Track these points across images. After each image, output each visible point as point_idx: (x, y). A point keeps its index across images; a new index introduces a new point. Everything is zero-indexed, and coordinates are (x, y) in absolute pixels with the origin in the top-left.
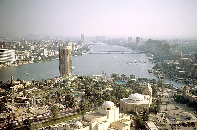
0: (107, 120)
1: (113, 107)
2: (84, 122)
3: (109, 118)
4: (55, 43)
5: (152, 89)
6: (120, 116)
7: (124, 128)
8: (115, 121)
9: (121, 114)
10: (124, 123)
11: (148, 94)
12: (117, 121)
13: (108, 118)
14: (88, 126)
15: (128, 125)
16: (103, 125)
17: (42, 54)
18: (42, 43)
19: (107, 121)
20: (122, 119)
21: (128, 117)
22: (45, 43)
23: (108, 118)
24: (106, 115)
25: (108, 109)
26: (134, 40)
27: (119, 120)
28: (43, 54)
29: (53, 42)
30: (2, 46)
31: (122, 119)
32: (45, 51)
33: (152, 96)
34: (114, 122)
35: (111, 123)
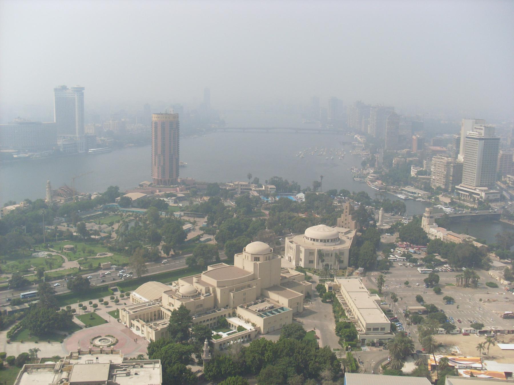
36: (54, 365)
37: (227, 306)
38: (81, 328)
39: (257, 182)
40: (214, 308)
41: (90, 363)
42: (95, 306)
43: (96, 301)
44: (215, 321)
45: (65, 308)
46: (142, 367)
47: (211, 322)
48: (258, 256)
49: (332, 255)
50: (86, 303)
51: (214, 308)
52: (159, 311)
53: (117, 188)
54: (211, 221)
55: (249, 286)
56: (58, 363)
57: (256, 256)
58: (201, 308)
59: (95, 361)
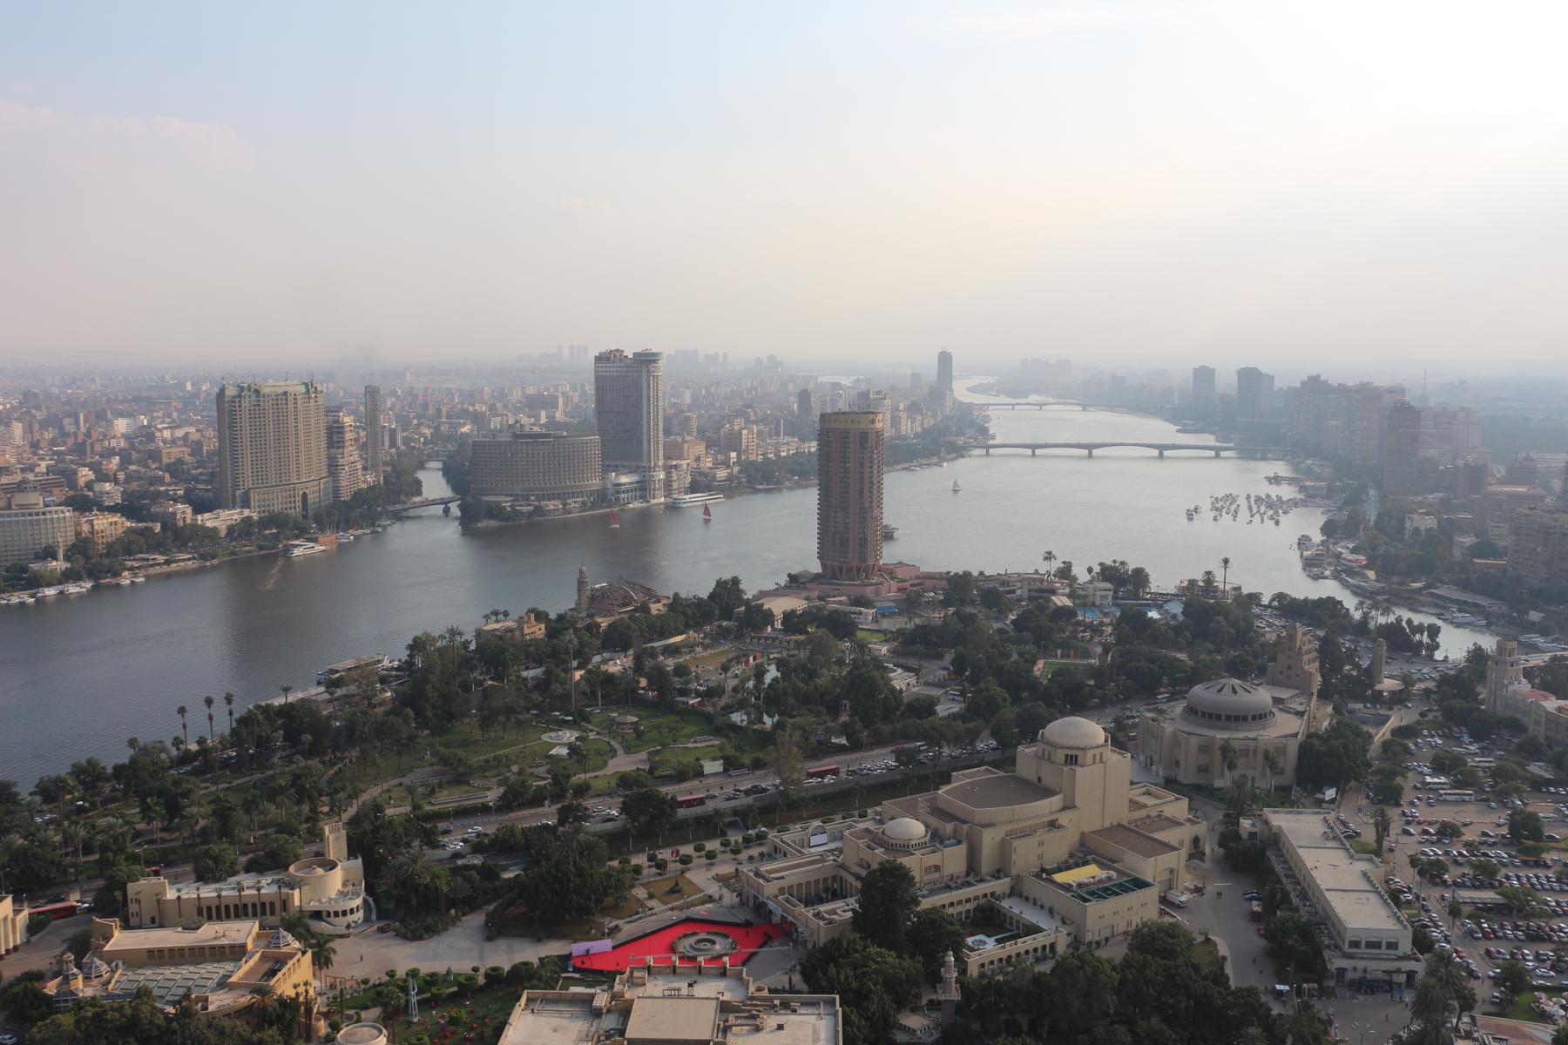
0: (1063, 819)
1: (1097, 752)
2: (934, 822)
3: (1074, 807)
4: (804, 396)
6: (1131, 801)
8: (1107, 825)
9: (1136, 794)
10: (1158, 836)
11: (1298, 683)
12: (1119, 825)
13: (1068, 806)
14: (959, 842)
15: (1174, 849)
16: (1041, 844)
17: (733, 455)
20: (1141, 814)
21: (1178, 807)
25: (1072, 760)
26: (1226, 381)
28: (739, 456)
30: (543, 414)
31: (1141, 814)
34: (1098, 826)
35: (1083, 834)
36: (593, 996)
37: (998, 871)
39: (1065, 572)
41: (674, 995)
42: (686, 860)
43: (687, 850)
44: (969, 906)
45: (615, 863)
46: (794, 1011)
47: (960, 908)
48: (1074, 753)
49: (1255, 755)
50: (665, 854)
51: (968, 874)
52: (834, 878)
53: (735, 581)
54: (959, 665)
55: (1053, 825)
57: (1070, 752)
58: (937, 875)
59: (685, 992)
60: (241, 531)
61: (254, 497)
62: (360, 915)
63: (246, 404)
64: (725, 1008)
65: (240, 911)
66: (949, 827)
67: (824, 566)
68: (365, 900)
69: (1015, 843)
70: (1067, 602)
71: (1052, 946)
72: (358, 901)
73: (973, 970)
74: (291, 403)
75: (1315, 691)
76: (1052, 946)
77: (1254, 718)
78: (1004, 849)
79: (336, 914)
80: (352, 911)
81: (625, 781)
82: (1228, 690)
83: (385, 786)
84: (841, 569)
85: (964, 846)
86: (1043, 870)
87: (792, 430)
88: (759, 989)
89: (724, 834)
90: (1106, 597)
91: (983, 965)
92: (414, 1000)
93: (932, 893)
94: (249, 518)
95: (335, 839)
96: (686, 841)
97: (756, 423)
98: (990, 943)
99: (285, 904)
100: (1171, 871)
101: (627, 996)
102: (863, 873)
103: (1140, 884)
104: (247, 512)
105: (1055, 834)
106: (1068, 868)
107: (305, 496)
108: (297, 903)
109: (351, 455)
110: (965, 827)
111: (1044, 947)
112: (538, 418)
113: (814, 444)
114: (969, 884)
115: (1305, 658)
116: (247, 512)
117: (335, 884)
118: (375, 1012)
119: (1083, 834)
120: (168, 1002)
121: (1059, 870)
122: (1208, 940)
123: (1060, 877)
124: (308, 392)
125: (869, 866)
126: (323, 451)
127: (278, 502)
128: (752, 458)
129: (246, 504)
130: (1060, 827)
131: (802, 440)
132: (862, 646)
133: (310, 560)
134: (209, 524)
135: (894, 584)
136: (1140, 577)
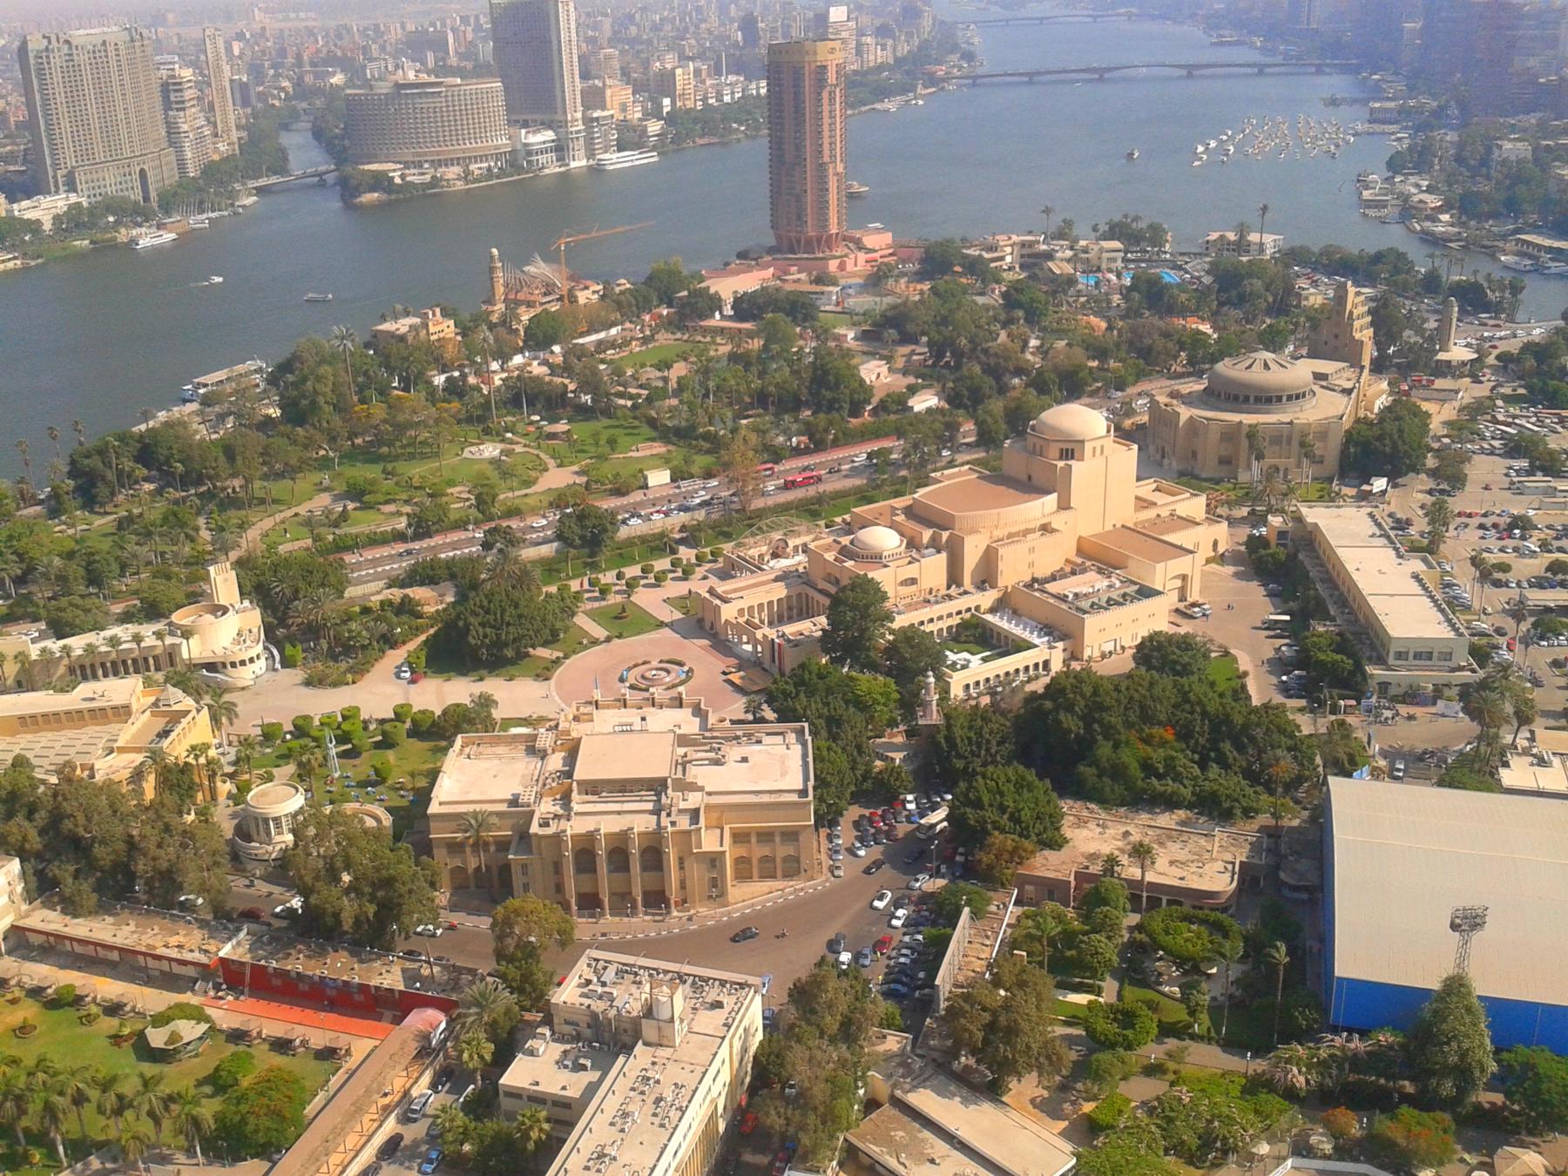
1: (1098, 444)
3: (1068, 508)
4: (748, 24)
5: (1372, 324)
7: (1160, 567)
8: (1109, 527)
10: (1165, 538)
11: (1347, 352)
14: (939, 552)
17: (667, 101)
18: (668, 27)
19: (1054, 526)
20: (1150, 514)
22: (686, 29)
23: (1064, 505)
24: (1048, 492)
27: (1131, 517)
28: (673, 103)
29: (732, 20)
31: (1150, 514)
32: (683, 77)
33: (1366, 371)
38: (595, 642)
40: (949, 587)
43: (632, 571)
45: (553, 589)
48: (1069, 446)
49: (1289, 442)
50: (608, 577)
51: (949, 587)
52: (799, 595)
55: (1046, 529)
56: (542, 730)
57: (1065, 446)
59: (637, 727)
60: (72, 222)
61: (79, 177)
62: (261, 665)
63: (57, 60)
64: (683, 740)
65: (117, 667)
66: (927, 535)
67: (779, 238)
68: (266, 648)
69: (1001, 552)
70: (1068, 269)
71: (1046, 664)
72: (259, 648)
73: (956, 691)
74: (111, 53)
75: (1366, 362)
76: (1046, 664)
77: (1290, 398)
78: (989, 560)
79: (233, 665)
80: (251, 660)
81: (558, 500)
82: (1258, 366)
83: (279, 517)
84: (799, 241)
85: (944, 555)
86: (1034, 580)
87: (738, 67)
88: (722, 721)
89: (674, 551)
90: (1114, 260)
91: (967, 686)
92: (333, 752)
93: (911, 607)
94: (79, 203)
95: (223, 581)
96: (631, 561)
97: (692, 59)
98: (975, 660)
99: (172, 654)
100: (1184, 578)
101: (574, 735)
102: (833, 590)
103: (1146, 593)
104: (73, 198)
105: (1049, 539)
106: (1064, 576)
107: (142, 173)
108: (185, 655)
109: (191, 120)
110: (945, 535)
111: (1036, 666)
112: (423, 62)
113: (763, 83)
114: (950, 597)
115: (1357, 324)
116: (73, 198)
117: (228, 630)
118: (291, 768)
119: (1080, 538)
120: (47, 772)
121: (1053, 578)
122: (1227, 653)
123: (1052, 587)
124: (132, 40)
125: (837, 581)
126: (160, 116)
127: (112, 182)
128: (690, 104)
129: (72, 187)
130: (1053, 531)
131: (749, 79)
132: (823, 334)
133: (157, 250)
134: (29, 215)
135: (862, 256)
136: (1155, 235)
